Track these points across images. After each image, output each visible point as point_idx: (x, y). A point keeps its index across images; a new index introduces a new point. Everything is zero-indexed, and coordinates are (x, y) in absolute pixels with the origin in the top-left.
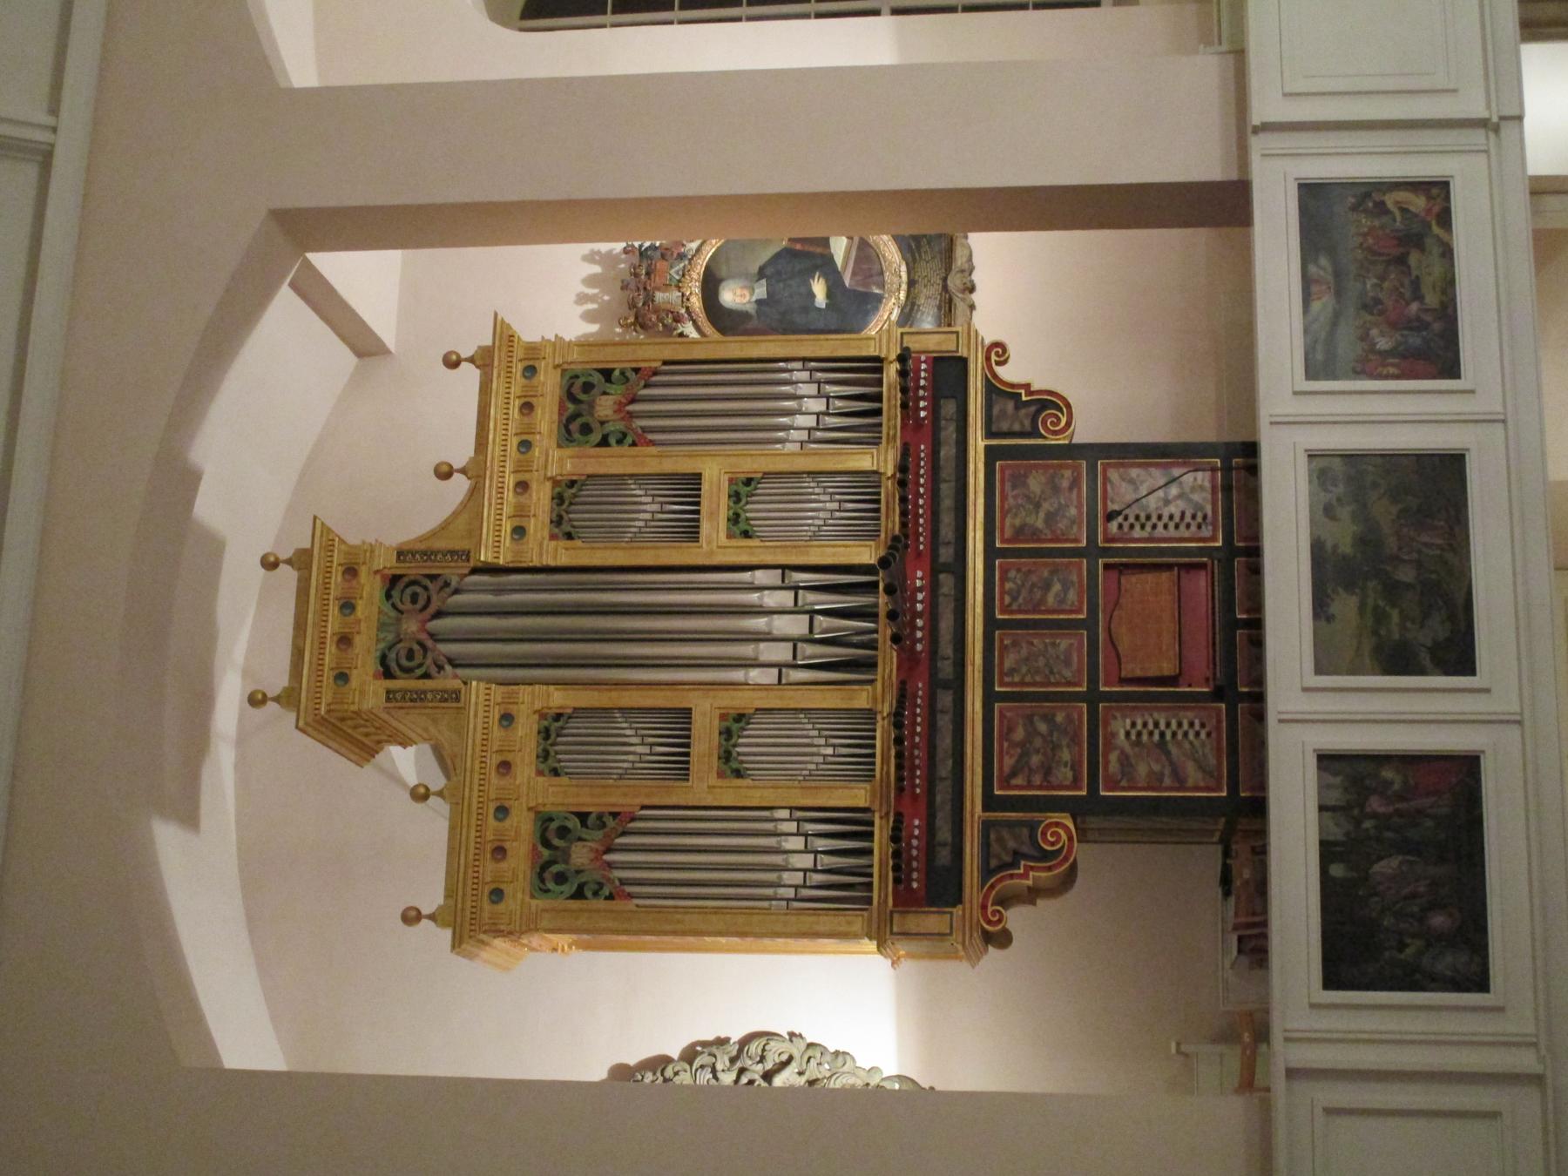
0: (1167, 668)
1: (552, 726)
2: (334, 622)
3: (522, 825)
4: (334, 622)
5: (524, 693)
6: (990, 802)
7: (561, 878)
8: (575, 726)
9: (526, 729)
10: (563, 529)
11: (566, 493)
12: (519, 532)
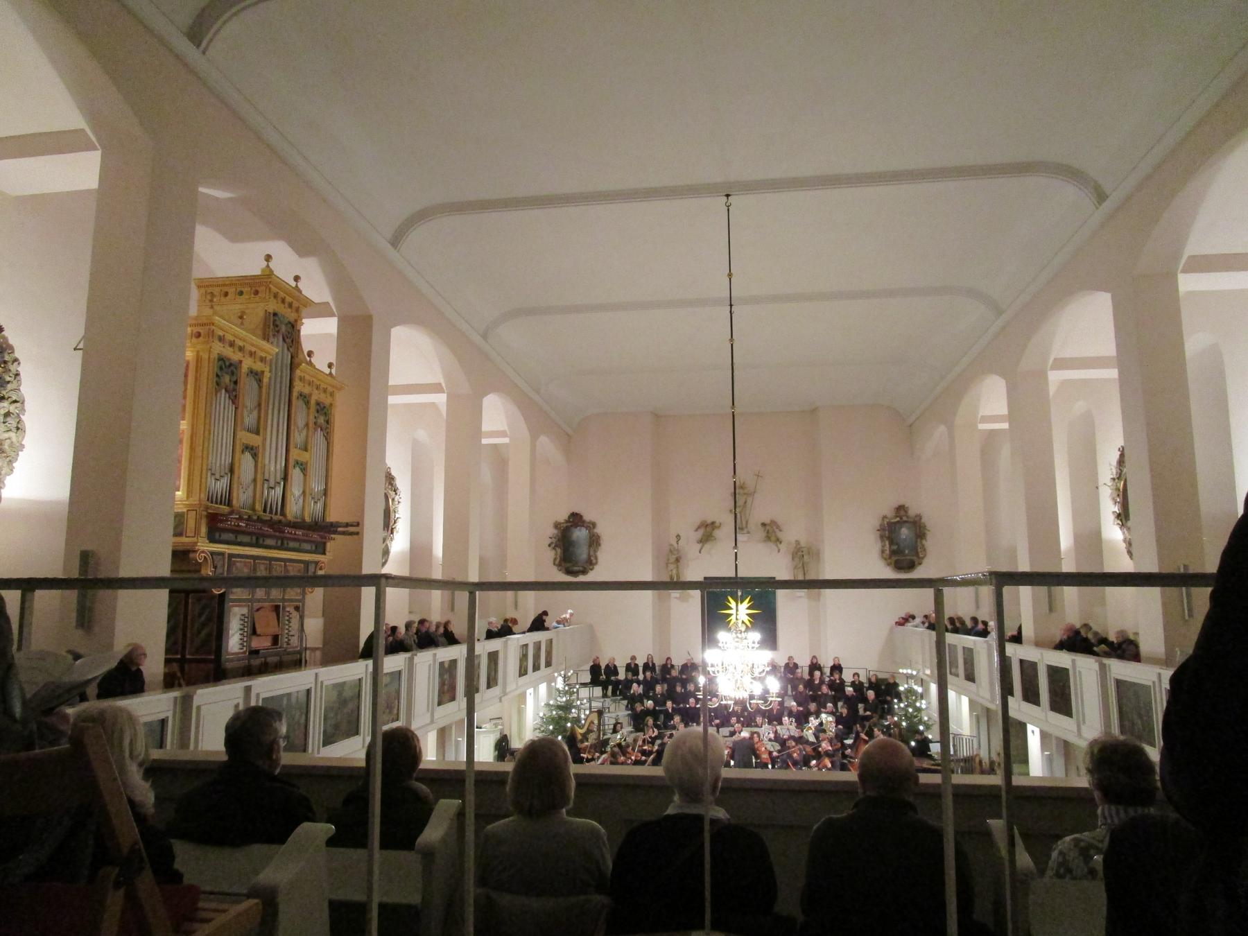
0: (258, 631)
1: (257, 376)
2: (288, 299)
3: (235, 356)
4: (288, 299)
5: (267, 369)
6: (231, 556)
7: (221, 368)
8: (255, 385)
9: (258, 366)
10: (301, 395)
11: (305, 398)
12: (301, 379)
